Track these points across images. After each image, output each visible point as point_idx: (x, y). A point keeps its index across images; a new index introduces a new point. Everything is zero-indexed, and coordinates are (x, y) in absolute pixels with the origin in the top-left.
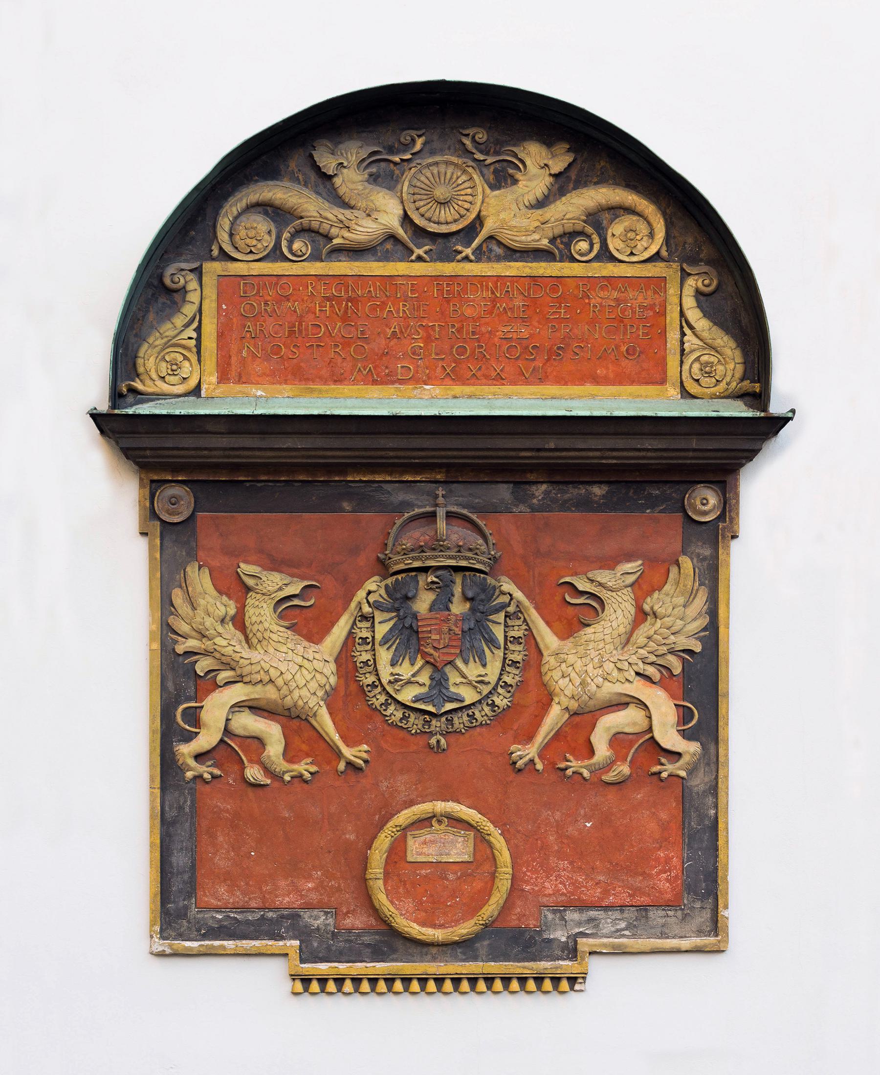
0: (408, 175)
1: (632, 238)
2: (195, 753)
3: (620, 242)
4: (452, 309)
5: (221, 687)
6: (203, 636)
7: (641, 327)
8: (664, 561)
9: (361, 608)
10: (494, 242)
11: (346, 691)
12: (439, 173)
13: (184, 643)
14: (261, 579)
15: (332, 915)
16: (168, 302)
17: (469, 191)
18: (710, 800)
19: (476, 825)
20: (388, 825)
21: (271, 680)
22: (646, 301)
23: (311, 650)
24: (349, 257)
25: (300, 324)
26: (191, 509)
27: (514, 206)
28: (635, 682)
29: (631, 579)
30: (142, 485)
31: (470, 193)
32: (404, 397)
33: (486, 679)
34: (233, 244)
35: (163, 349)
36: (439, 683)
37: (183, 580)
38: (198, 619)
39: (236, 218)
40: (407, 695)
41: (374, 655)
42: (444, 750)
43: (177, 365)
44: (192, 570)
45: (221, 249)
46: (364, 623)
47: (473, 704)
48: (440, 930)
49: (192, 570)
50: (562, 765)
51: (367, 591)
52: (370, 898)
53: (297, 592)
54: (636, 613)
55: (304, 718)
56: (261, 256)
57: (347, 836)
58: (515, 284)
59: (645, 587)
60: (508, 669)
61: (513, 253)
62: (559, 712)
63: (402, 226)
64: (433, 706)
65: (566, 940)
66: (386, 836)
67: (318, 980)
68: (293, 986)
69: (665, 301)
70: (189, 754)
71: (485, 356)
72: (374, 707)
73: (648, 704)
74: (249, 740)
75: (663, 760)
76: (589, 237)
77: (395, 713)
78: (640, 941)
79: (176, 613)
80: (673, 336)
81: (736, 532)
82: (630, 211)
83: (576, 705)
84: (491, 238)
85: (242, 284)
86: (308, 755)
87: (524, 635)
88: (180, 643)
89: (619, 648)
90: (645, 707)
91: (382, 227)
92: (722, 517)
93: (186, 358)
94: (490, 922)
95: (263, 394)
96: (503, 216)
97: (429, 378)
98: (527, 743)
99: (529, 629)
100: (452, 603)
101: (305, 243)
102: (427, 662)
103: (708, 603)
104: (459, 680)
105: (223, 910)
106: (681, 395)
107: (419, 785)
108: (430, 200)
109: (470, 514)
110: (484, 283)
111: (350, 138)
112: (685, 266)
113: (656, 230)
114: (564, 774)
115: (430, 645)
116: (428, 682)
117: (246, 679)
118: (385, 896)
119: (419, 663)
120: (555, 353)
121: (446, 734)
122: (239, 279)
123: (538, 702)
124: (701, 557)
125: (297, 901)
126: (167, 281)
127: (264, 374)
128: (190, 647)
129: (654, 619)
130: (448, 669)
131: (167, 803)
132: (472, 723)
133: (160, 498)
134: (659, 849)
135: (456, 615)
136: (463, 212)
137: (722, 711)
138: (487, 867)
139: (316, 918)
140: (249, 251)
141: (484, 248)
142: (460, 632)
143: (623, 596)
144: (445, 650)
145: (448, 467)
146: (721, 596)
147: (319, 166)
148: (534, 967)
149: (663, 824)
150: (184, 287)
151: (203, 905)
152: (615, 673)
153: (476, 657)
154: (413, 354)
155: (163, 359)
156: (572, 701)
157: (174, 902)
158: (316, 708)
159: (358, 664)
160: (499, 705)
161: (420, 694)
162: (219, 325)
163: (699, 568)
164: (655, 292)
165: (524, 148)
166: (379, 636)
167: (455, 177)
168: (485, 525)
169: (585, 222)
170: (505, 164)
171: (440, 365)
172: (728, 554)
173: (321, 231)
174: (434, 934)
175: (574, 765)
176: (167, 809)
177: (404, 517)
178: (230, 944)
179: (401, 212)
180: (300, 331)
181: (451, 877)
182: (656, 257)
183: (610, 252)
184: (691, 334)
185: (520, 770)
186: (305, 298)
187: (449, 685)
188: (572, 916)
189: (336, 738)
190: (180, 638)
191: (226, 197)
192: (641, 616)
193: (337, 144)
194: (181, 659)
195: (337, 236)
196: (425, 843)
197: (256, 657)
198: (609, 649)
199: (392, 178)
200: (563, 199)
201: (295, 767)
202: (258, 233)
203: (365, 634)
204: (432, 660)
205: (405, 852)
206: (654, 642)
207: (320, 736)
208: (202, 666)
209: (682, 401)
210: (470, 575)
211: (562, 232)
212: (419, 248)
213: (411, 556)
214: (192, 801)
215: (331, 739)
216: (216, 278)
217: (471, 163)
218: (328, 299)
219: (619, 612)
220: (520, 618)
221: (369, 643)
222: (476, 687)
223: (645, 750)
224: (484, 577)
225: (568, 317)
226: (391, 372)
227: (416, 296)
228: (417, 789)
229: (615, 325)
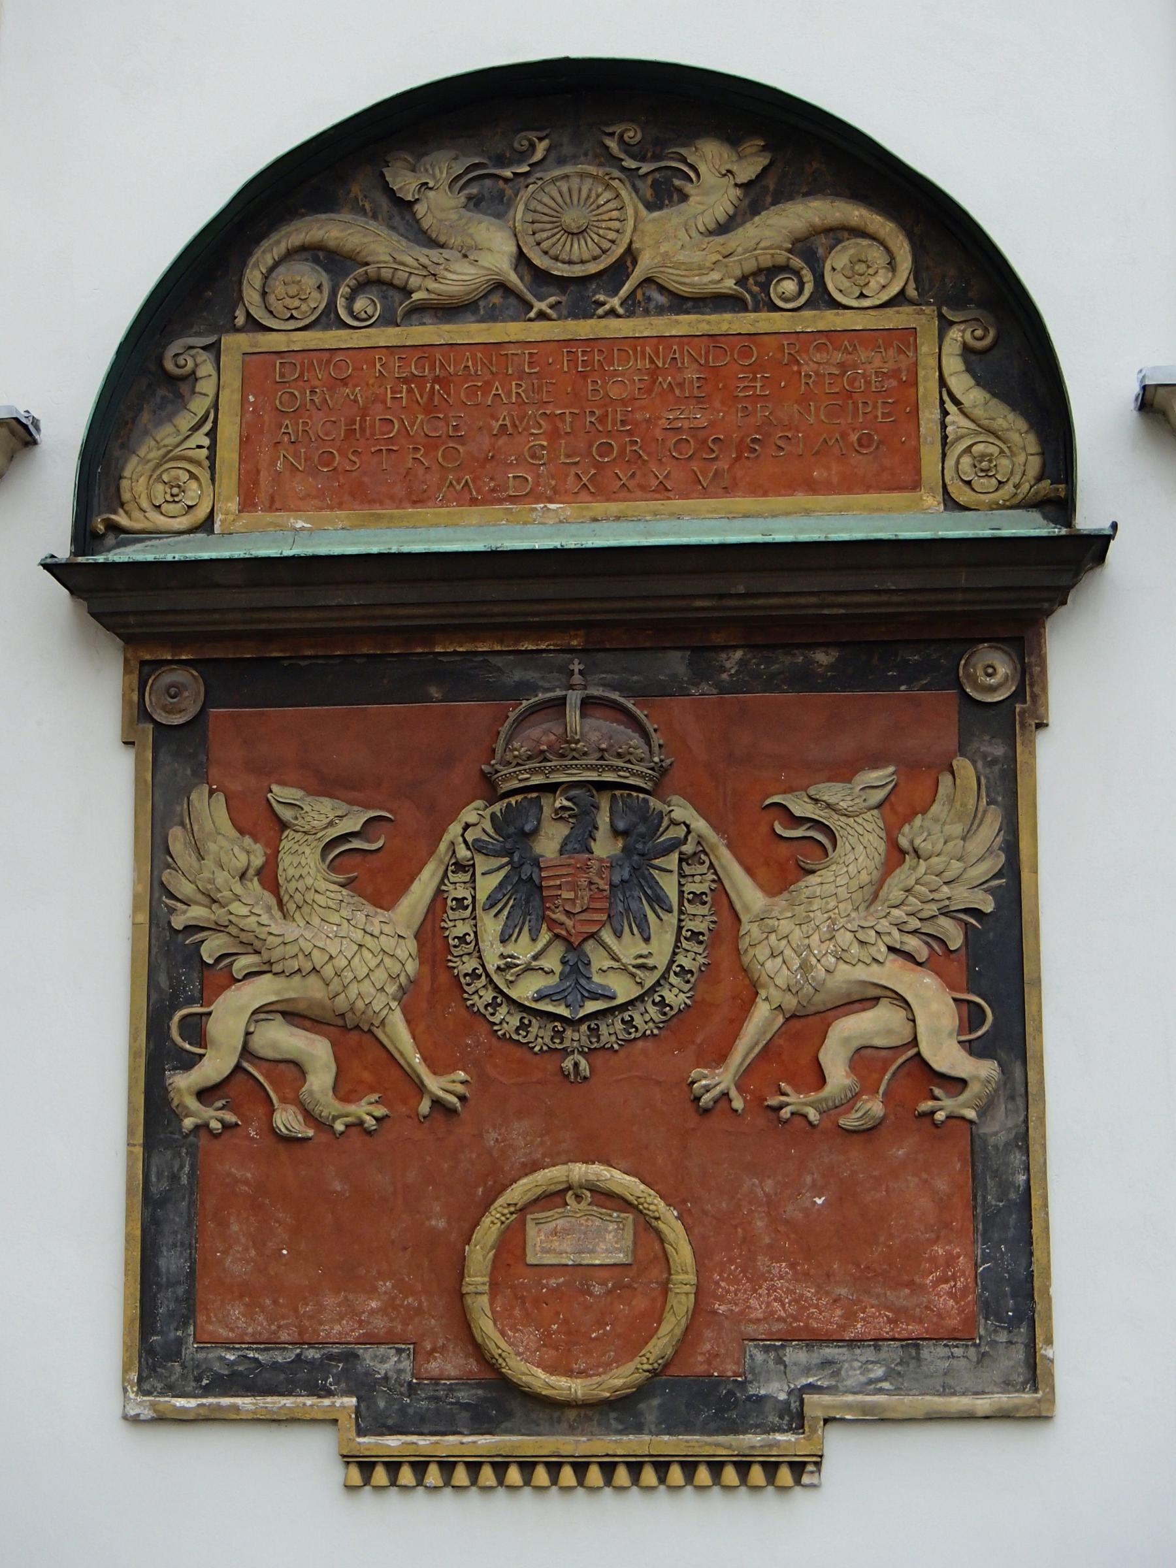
0: (525, 194)
1: (861, 271)
2: (198, 1087)
3: (844, 279)
4: (590, 388)
5: (239, 981)
7: (879, 405)
8: (929, 767)
9: (454, 852)
10: (654, 287)
11: (432, 984)
12: (570, 191)
13: (185, 912)
14: (302, 809)
15: (409, 1355)
16: (170, 396)
17: (615, 214)
18: (1017, 1158)
19: (636, 1203)
20: (496, 1204)
21: (314, 968)
22: (886, 365)
23: (378, 920)
24: (437, 317)
25: (363, 420)
26: (200, 704)
27: (682, 234)
28: (888, 964)
29: (878, 796)
30: (127, 670)
31: (615, 217)
32: (518, 523)
33: (650, 962)
34: (266, 307)
35: (159, 465)
37: (186, 814)
38: (206, 874)
39: (271, 270)
40: (525, 990)
41: (475, 926)
42: (585, 1078)
43: (179, 486)
44: (199, 797)
45: (249, 315)
46: (460, 875)
47: (631, 1003)
48: (579, 1381)
49: (199, 797)
50: (773, 1101)
51: (463, 824)
52: (469, 1326)
53: (357, 828)
54: (888, 852)
55: (366, 1030)
56: (307, 322)
57: (433, 1223)
58: (686, 347)
59: (900, 809)
60: (685, 944)
61: (681, 303)
62: (767, 1014)
63: (516, 269)
64: (568, 1006)
65: (786, 1397)
66: (493, 1222)
67: (386, 1464)
68: (346, 1474)
69: (916, 364)
70: (188, 1088)
71: (640, 456)
72: (475, 1009)
74: (282, 1066)
75: (937, 1092)
76: (797, 273)
78: (907, 1399)
79: (174, 865)
80: (929, 416)
81: (1042, 717)
83: (794, 1002)
84: (649, 281)
85: (278, 364)
86: (372, 1090)
87: (711, 890)
88: (178, 913)
90: (907, 1005)
91: (484, 272)
92: (1018, 695)
93: (193, 476)
94: (661, 1367)
95: (306, 525)
96: (662, 250)
97: (555, 491)
98: (718, 1066)
99: (719, 880)
100: (595, 840)
101: (373, 301)
102: (557, 936)
103: (1002, 832)
104: (608, 963)
105: (237, 1346)
106: (945, 505)
107: (546, 1138)
108: (556, 230)
109: (622, 700)
110: (639, 348)
111: (440, 149)
112: (944, 310)
113: (898, 259)
114: (779, 1118)
115: (561, 908)
116: (558, 968)
117: (277, 968)
118: (491, 1323)
119: (545, 937)
120: (746, 449)
121: (588, 1053)
122: (273, 357)
123: (734, 998)
124: (989, 759)
125: (353, 1331)
126: (169, 365)
127: (309, 495)
128: (194, 918)
129: (916, 860)
130: (590, 947)
131: (154, 1170)
133: (155, 687)
134: (936, 1241)
135: (601, 860)
136: (606, 245)
137: (1029, 1009)
138: (655, 1272)
139: (383, 1360)
141: (639, 296)
142: (607, 887)
143: (865, 824)
144: (584, 916)
145: (588, 625)
146: (1022, 820)
147: (392, 189)
148: (734, 1443)
149: (942, 1199)
150: (194, 372)
151: (205, 1337)
152: (855, 949)
153: (633, 925)
154: (533, 456)
155: (160, 476)
156: (788, 996)
157: (161, 1333)
158: (385, 1012)
159: (451, 941)
160: (671, 1003)
161: (546, 987)
162: (244, 426)
163: (987, 778)
164: (900, 351)
165: (697, 149)
166: (482, 897)
167: (593, 195)
168: (646, 716)
169: (790, 251)
170: (669, 173)
171: (573, 473)
172: (1032, 754)
173: (396, 282)
174: (570, 1387)
175: (794, 1100)
176: (154, 1179)
177: (521, 707)
178: (245, 1403)
179: (514, 249)
180: (363, 430)
181: (597, 1290)
182: (899, 299)
184: (958, 412)
185: (706, 1111)
186: (371, 382)
187: (591, 973)
188: (795, 1355)
189: (417, 1060)
190: (179, 904)
192: (896, 855)
193: (419, 157)
194: (180, 937)
195: (419, 289)
196: (555, 1233)
197: (293, 931)
198: (846, 910)
199: (502, 201)
200: (757, 219)
201: (352, 1108)
202: (302, 289)
204: (564, 933)
205: (524, 1249)
206: (916, 897)
207: (391, 1059)
208: (211, 948)
209: (946, 514)
210: (622, 795)
211: (756, 269)
212: (541, 299)
213: (527, 767)
214: (193, 1167)
215: (409, 1064)
216: (240, 357)
217: (616, 173)
218: (406, 381)
220: (704, 862)
221: (467, 907)
222: (633, 975)
223: (909, 1074)
224: (644, 799)
225: (767, 393)
226: (499, 486)
227: (535, 370)
228: (542, 1143)
229: (840, 403)
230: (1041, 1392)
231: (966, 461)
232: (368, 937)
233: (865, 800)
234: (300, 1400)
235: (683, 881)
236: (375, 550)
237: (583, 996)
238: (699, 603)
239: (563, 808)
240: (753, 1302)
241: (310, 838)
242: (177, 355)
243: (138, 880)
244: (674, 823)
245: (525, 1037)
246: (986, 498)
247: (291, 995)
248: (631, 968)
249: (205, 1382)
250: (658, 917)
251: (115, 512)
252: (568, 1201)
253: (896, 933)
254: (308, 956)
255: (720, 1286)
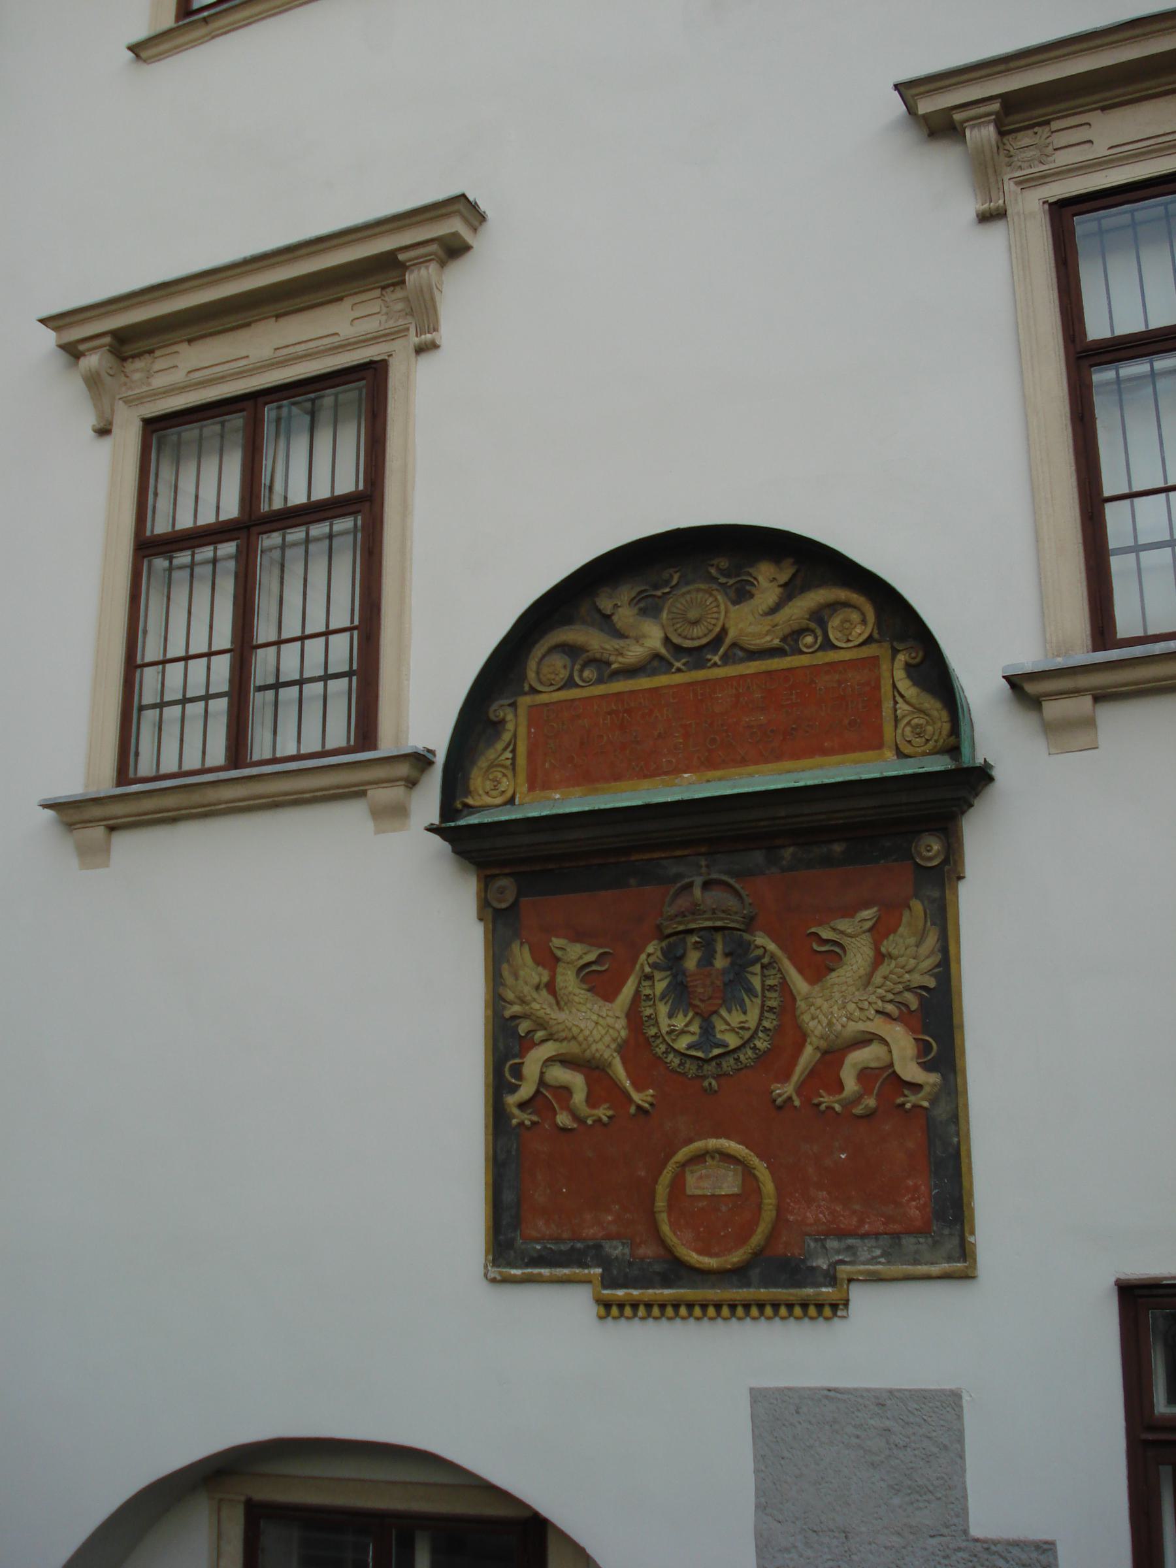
3: (838, 632)
6: (522, 1001)
9: (643, 970)
18: (952, 1128)
23: (605, 1008)
28: (876, 1020)
29: (868, 925)
30: (479, 881)
33: (746, 1025)
36: (708, 1030)
40: (682, 1044)
41: (655, 1009)
42: (716, 1091)
44: (516, 947)
50: (815, 1101)
56: (559, 685)
57: (639, 1173)
60: (766, 1014)
61: (754, 655)
64: (703, 1052)
66: (667, 1173)
73: (888, 1039)
75: (906, 1092)
76: (813, 631)
77: (675, 1060)
80: (887, 706)
82: (846, 605)
83: (825, 1044)
84: (734, 645)
89: (861, 989)
90: (886, 1043)
91: (646, 650)
92: (946, 861)
96: (741, 626)
99: (783, 978)
100: (715, 959)
104: (724, 1027)
112: (895, 644)
117: (556, 1037)
119: (690, 1014)
121: (717, 1077)
128: (515, 1012)
130: (714, 1018)
132: (738, 1065)
135: (718, 970)
139: (615, 1249)
140: (549, 684)
143: (862, 941)
146: (951, 933)
152: (857, 1013)
158: (610, 1059)
169: (809, 620)
175: (826, 1100)
178: (545, 1272)
181: (724, 1209)
182: (869, 640)
183: (830, 640)
185: (780, 1108)
188: (832, 1244)
189: (628, 1084)
190: (509, 1006)
191: (536, 642)
192: (880, 958)
195: (615, 662)
196: (701, 1177)
200: (790, 604)
201: (595, 1112)
203: (648, 991)
204: (700, 1011)
207: (615, 1085)
208: (523, 1027)
212: (678, 660)
217: (715, 586)
218: (609, 713)
219: (859, 956)
221: (652, 999)
222: (737, 1033)
230: (968, 1263)
231: (908, 729)
232: (600, 1019)
233: (861, 928)
234: (573, 1270)
235: (764, 979)
236: (587, 809)
237: (711, 1045)
238: (762, 823)
239: (697, 942)
240: (808, 1214)
241: (571, 966)
242: (495, 711)
243: (486, 993)
244: (758, 947)
245: (683, 1069)
246: (919, 750)
247: (563, 1051)
248: (737, 1030)
249: (526, 1260)
250: (752, 1001)
251: (466, 797)
252: (707, 1160)
253: (880, 1003)
254: (570, 1030)
255: (790, 1206)
